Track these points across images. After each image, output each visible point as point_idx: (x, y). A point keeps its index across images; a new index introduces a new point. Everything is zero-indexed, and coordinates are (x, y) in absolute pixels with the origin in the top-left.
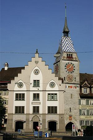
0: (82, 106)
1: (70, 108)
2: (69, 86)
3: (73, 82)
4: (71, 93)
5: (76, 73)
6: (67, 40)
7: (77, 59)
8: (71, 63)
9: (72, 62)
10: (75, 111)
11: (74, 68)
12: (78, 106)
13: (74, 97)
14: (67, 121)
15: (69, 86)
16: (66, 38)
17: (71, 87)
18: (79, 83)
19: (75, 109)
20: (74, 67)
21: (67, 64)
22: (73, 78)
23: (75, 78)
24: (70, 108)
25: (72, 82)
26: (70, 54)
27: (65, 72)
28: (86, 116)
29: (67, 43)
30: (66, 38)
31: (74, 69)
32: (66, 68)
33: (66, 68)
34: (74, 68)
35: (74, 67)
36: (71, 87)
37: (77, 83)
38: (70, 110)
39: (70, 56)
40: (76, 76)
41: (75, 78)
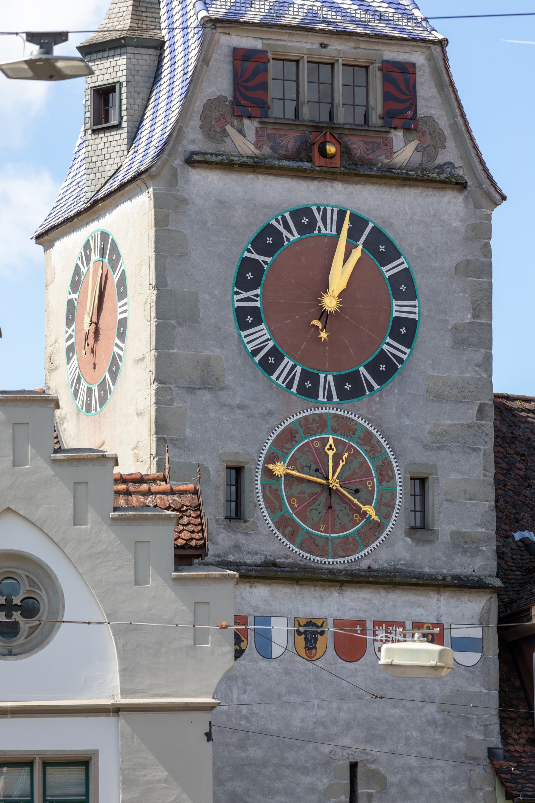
5: (439, 397)
11: (399, 308)
18: (482, 563)
20: (404, 285)
21: (267, 240)
22: (385, 472)
23: (420, 483)
25: (365, 558)
27: (243, 384)
32: (255, 297)
33: (255, 297)
34: (399, 308)
40: (439, 442)
41: (420, 483)
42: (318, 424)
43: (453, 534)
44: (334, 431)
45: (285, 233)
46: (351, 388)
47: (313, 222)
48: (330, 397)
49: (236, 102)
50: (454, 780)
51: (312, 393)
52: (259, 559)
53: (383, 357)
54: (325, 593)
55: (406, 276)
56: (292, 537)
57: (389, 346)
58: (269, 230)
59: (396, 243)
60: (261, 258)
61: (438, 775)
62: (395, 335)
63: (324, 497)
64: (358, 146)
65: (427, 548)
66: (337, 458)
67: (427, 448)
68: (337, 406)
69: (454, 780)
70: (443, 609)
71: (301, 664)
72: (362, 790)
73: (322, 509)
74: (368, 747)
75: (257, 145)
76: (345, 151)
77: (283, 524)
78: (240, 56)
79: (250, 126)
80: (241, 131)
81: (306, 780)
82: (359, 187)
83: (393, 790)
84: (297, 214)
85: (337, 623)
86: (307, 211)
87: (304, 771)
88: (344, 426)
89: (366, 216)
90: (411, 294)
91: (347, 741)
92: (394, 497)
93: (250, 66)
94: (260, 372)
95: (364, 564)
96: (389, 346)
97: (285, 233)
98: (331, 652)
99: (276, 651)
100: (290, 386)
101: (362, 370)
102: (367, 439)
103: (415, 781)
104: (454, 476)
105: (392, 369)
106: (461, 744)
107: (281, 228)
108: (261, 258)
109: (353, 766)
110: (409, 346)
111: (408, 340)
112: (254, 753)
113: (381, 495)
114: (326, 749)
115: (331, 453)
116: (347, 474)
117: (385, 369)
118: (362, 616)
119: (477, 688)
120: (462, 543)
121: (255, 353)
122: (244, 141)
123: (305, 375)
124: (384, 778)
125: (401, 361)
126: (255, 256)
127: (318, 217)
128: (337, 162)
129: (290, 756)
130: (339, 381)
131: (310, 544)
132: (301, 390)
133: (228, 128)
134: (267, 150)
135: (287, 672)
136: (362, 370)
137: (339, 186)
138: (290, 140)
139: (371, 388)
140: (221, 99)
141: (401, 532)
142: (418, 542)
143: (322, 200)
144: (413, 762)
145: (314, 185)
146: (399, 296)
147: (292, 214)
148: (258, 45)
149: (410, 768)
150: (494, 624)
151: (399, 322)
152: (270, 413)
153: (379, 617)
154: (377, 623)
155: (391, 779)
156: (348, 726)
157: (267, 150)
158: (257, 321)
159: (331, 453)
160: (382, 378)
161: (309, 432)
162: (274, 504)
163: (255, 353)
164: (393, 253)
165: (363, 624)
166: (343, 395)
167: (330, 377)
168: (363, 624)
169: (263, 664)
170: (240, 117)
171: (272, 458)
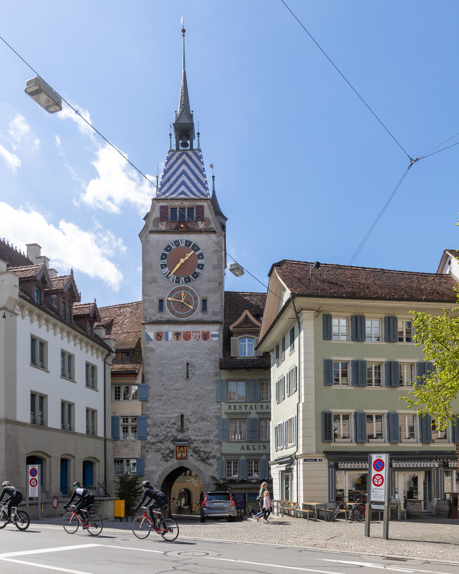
0: (232, 405)
1: (182, 416)
2: (177, 335)
3: (198, 315)
4: (187, 359)
5: (209, 281)
6: (184, 162)
7: (212, 225)
8: (188, 243)
9: (193, 238)
10: (202, 424)
11: (200, 262)
12: (214, 407)
13: (197, 373)
14: (170, 463)
15: (177, 335)
16: (180, 156)
17: (187, 336)
18: (220, 317)
19: (203, 419)
20: (201, 256)
21: (168, 248)
22: (196, 298)
24: (182, 416)
25: (191, 318)
26: (183, 209)
28: (245, 445)
29: (184, 172)
30: (180, 156)
31: (201, 267)
35: (201, 256)
36: (187, 336)
37: (206, 317)
38: (179, 423)
39: (182, 216)
41: (204, 301)
42: (181, 289)
43: (212, 311)
44: (184, 290)
45: (172, 247)
46: (188, 280)
47: (179, 244)
48: (183, 283)
49: (161, 218)
50: (211, 366)
51: (179, 282)
52: (166, 319)
53: (196, 273)
54: (181, 326)
55: (201, 254)
56: (174, 314)
57: (197, 270)
58: (169, 246)
59: (199, 247)
60: (167, 253)
61: (207, 365)
62: (199, 268)
63: (181, 305)
64: (190, 225)
65: (206, 315)
66: (184, 296)
67: (206, 292)
68: (184, 284)
69: (211, 366)
70: (209, 328)
71: (175, 342)
72: (189, 369)
73: (181, 307)
74: (191, 359)
75: (166, 227)
76: (186, 227)
77: (172, 311)
78: (162, 207)
79: (164, 223)
80: (162, 225)
81: (176, 367)
82: (190, 235)
83: (197, 368)
84: (175, 242)
85: (184, 332)
86: (178, 241)
87: (176, 365)
88: (186, 289)
89: (192, 241)
90: (203, 258)
91: (186, 358)
92: (198, 304)
93: (164, 209)
94: (166, 278)
95: (191, 319)
96: (197, 270)
97: (172, 247)
98: (182, 339)
99: (170, 339)
100: (173, 281)
101: (191, 276)
102: (192, 291)
103: (202, 366)
104: (212, 298)
105: (198, 275)
106: (213, 358)
107: (171, 246)
108: (167, 253)
109: (188, 364)
110: (202, 270)
111: (201, 269)
112: (164, 361)
113: (195, 304)
114: (181, 360)
115: (183, 295)
116: (187, 299)
117: (196, 275)
118: (190, 331)
119: (218, 345)
120: (214, 313)
121: (165, 274)
122: (163, 227)
123: (177, 278)
124: (195, 366)
125: (200, 273)
126: (165, 252)
127: (180, 242)
128: (184, 229)
129: (173, 362)
130: (185, 279)
131: (178, 315)
132: (176, 281)
133: (159, 224)
134: (168, 228)
135: (172, 344)
136: (191, 276)
137: (185, 235)
138: (174, 225)
139: (193, 280)
140: (158, 218)
141: (199, 312)
142: (204, 314)
143: (181, 238)
144: (202, 362)
145: (179, 235)
146: (199, 259)
147: (174, 242)
148: (166, 204)
149: (201, 364)
150: (221, 331)
151: (199, 265)
152: (169, 287)
153: (194, 331)
154: (193, 332)
155: (196, 366)
156: (186, 355)
157: (168, 228)
158: (166, 267)
159: (183, 295)
160: (195, 278)
161: (178, 291)
162: (169, 307)
163: (165, 274)
164: (198, 249)
165: (190, 332)
166: (186, 282)
167: (183, 278)
168: (190, 332)
169: (167, 342)
170: (162, 221)
171: (168, 297)
